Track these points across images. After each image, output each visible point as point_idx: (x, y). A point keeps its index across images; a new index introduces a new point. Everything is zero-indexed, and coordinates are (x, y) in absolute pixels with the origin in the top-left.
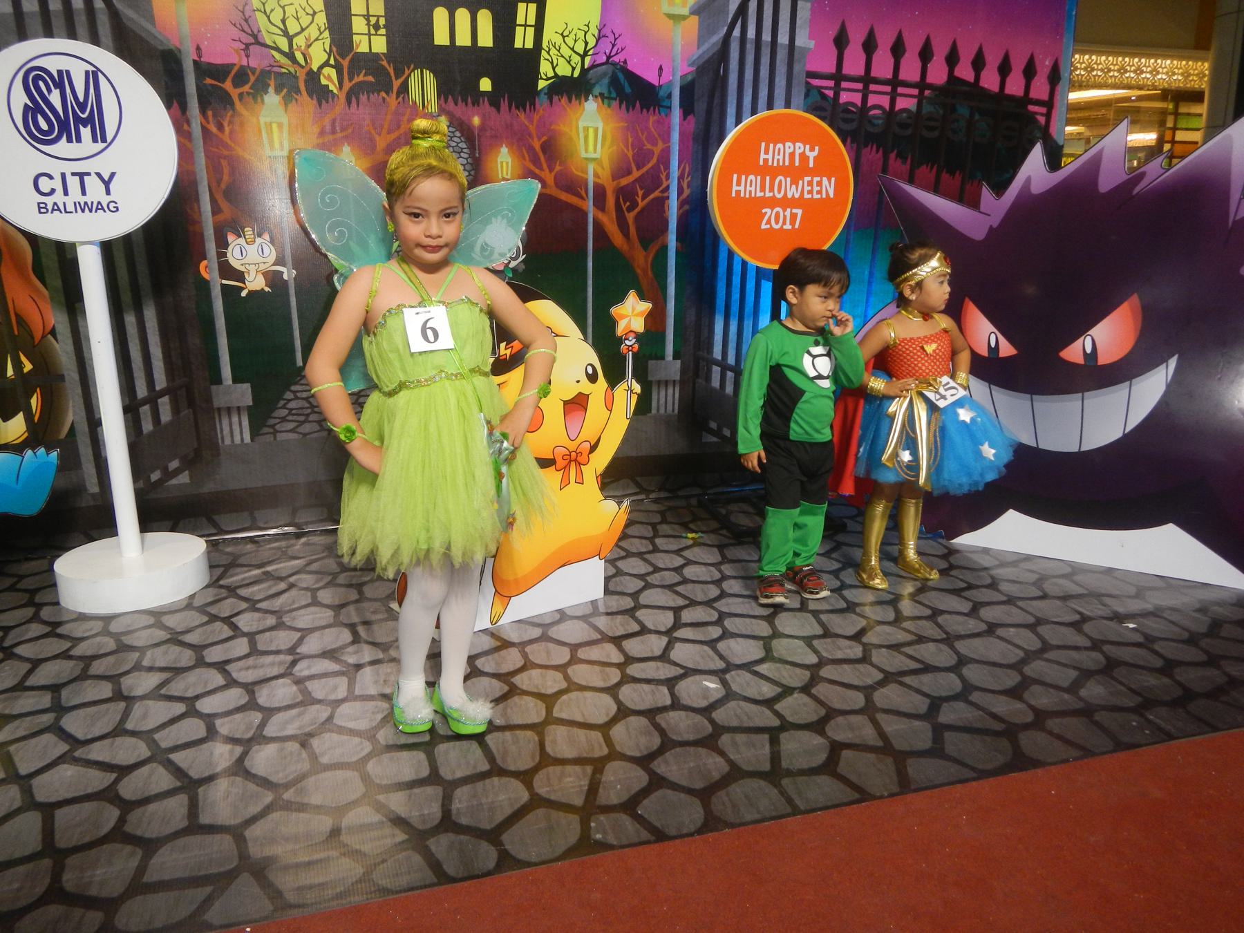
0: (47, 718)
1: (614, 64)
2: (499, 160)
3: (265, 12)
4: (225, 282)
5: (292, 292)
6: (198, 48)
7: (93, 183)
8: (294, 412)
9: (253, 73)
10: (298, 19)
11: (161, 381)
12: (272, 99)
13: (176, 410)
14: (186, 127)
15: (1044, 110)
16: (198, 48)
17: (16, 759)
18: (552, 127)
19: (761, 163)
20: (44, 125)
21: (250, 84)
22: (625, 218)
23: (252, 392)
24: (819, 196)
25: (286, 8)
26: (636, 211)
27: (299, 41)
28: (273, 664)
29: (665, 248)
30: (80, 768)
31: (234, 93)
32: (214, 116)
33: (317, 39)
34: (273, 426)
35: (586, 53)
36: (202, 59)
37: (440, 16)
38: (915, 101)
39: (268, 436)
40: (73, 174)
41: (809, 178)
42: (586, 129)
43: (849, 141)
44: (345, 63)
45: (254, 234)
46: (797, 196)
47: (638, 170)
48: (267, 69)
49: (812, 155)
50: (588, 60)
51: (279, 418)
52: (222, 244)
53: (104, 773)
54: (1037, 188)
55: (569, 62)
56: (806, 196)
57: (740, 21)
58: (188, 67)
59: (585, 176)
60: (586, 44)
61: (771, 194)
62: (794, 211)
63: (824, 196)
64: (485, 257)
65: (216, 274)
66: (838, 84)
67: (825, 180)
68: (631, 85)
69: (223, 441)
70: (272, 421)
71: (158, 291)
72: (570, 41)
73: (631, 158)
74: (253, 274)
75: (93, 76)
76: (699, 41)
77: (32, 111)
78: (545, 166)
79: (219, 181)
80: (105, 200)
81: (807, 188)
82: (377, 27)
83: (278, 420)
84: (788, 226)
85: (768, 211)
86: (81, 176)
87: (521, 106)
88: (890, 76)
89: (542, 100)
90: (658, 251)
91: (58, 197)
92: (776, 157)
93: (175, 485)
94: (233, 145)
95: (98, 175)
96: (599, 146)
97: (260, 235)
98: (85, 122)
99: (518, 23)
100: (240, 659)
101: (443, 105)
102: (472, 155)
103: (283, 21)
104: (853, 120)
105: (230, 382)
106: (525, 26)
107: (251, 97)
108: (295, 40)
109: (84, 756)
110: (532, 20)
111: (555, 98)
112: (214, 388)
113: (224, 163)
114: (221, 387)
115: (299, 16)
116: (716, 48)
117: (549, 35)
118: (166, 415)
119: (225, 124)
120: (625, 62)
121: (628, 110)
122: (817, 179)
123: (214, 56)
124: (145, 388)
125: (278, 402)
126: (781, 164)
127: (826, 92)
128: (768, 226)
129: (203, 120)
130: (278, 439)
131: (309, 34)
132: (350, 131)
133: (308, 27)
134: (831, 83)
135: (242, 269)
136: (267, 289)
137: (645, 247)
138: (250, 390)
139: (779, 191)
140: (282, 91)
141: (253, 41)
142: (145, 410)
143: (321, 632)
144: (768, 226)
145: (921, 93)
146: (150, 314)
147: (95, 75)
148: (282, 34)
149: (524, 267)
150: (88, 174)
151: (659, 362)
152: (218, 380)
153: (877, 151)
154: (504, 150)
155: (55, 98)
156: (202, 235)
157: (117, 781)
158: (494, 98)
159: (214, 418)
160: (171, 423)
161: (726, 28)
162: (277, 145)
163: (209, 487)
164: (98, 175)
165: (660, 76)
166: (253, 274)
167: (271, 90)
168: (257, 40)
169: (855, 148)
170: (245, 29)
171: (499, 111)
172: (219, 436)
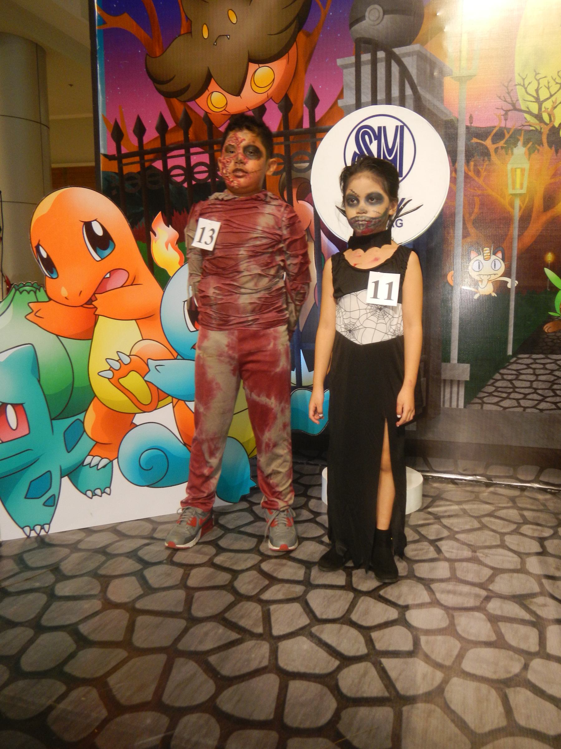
0: (299, 589)
3: (524, 86)
6: (471, 117)
8: (499, 389)
9: (508, 133)
10: (548, 88)
12: (520, 150)
16: (471, 117)
17: (273, 619)
21: (505, 140)
23: (471, 370)
25: (540, 81)
27: (548, 105)
28: (468, 595)
30: (314, 645)
32: (475, 165)
34: (481, 398)
36: (472, 125)
39: (477, 405)
45: (491, 252)
48: (520, 128)
51: (487, 393)
53: (330, 657)
58: (462, 132)
69: (444, 405)
70: (481, 395)
75: (400, 130)
79: (470, 214)
83: (486, 395)
97: (495, 254)
100: (442, 581)
103: (537, 91)
107: (503, 152)
108: (545, 105)
109: (318, 634)
112: (444, 364)
114: (448, 365)
115: (550, 85)
123: (480, 123)
125: (488, 381)
129: (466, 168)
130: (484, 408)
131: (556, 100)
133: (556, 93)
136: (494, 294)
138: (469, 369)
140: (528, 143)
141: (511, 107)
143: (510, 574)
147: (402, 128)
148: (534, 100)
152: (447, 359)
157: (339, 669)
159: (440, 387)
162: (518, 186)
166: (485, 282)
167: (520, 144)
168: (516, 108)
170: (507, 100)
172: (442, 400)
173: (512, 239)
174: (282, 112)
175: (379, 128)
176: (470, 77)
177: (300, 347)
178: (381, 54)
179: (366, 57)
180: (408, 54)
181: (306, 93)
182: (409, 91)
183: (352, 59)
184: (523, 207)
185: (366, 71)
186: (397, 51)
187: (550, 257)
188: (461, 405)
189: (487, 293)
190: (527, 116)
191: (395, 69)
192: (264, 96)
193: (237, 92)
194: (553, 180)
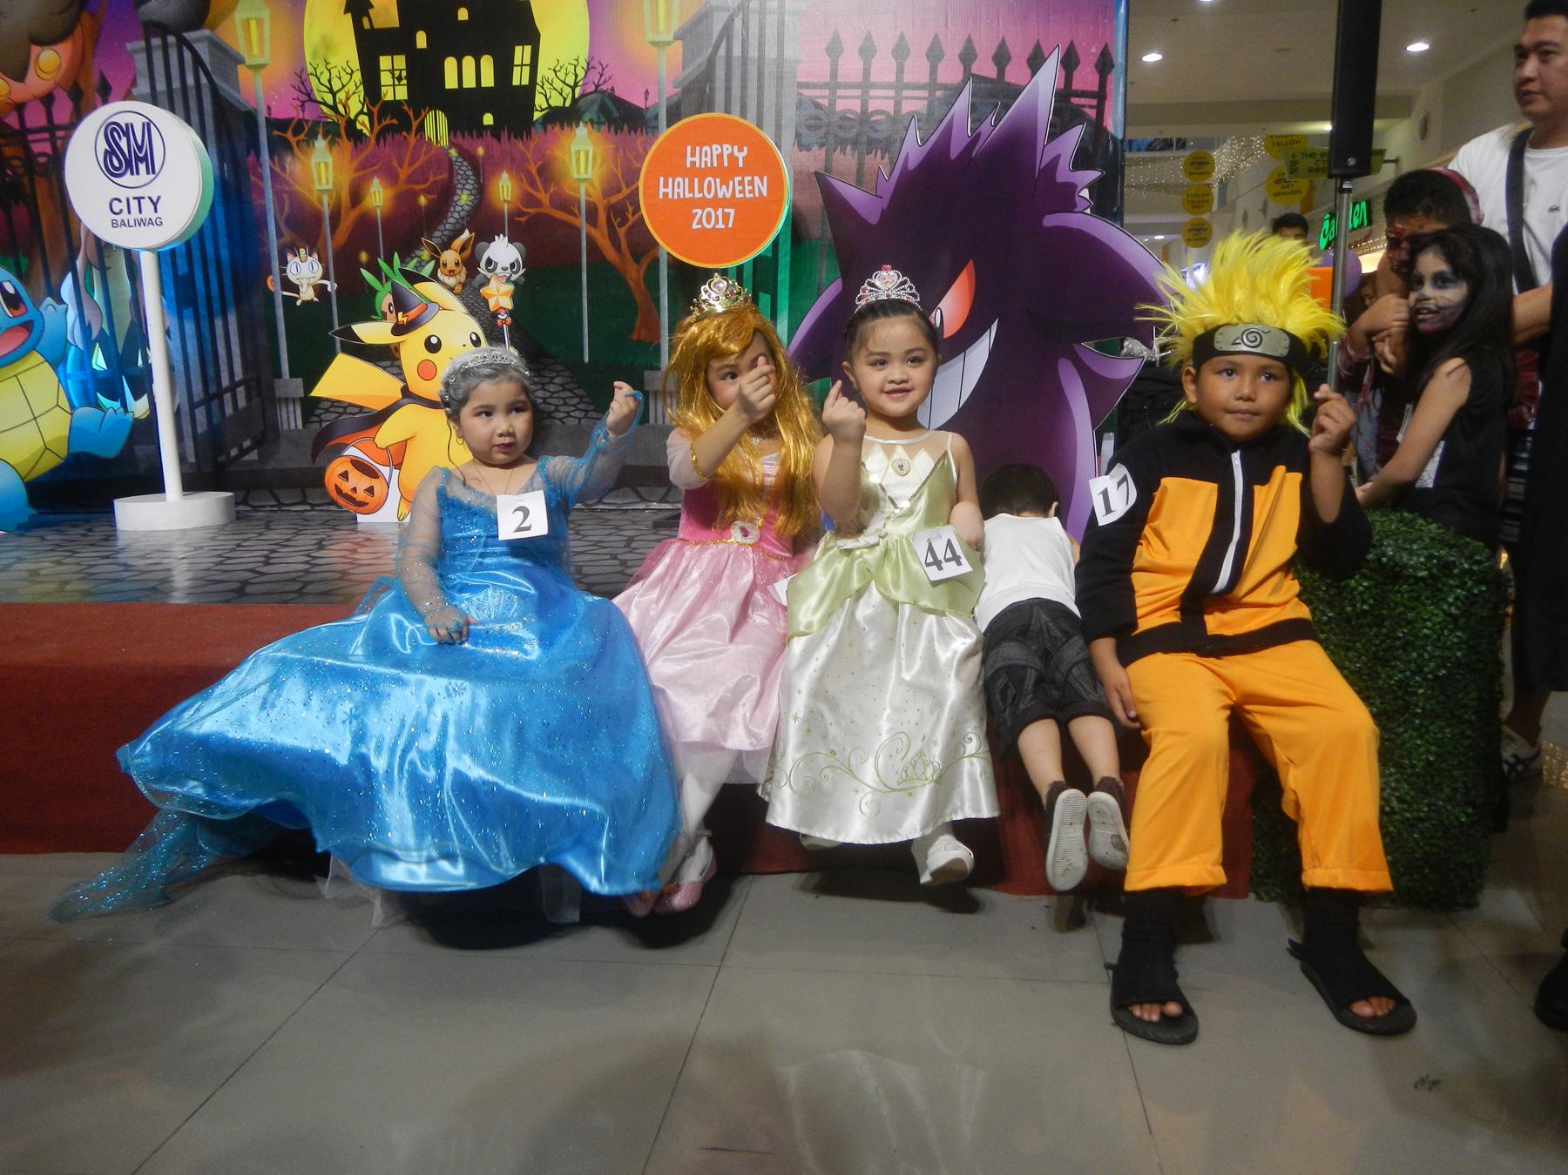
1: (604, 92)
2: (500, 184)
4: (285, 293)
5: (334, 301)
6: (269, 108)
7: (146, 204)
11: (239, 376)
12: (321, 144)
13: (249, 398)
14: (259, 170)
15: (1094, 102)
18: (548, 152)
19: (688, 165)
20: (117, 164)
22: (616, 233)
24: (752, 195)
26: (627, 226)
27: (341, 96)
29: (656, 261)
31: (293, 140)
33: (354, 93)
34: (318, 416)
35: (576, 84)
37: (450, 64)
38: (926, 102)
40: (135, 198)
41: (740, 178)
42: (578, 152)
43: (849, 147)
44: (375, 110)
46: (728, 195)
47: (628, 187)
49: (741, 156)
50: (578, 91)
52: (284, 262)
54: (912, 165)
55: (561, 94)
56: (738, 196)
57: (724, 41)
59: (577, 195)
60: (576, 76)
61: (701, 195)
62: (726, 210)
63: (757, 195)
64: (490, 271)
65: (279, 286)
66: (833, 93)
67: (757, 179)
68: (618, 109)
70: (318, 412)
71: (239, 300)
72: (561, 75)
73: (620, 175)
74: (305, 286)
75: (147, 126)
76: (683, 63)
77: (109, 153)
78: (540, 186)
79: (282, 210)
80: (154, 216)
81: (738, 188)
82: (400, 79)
84: (721, 226)
85: (699, 211)
86: (139, 199)
87: (519, 135)
88: (892, 78)
89: (537, 131)
90: (649, 265)
91: (125, 216)
92: (704, 159)
93: (247, 461)
94: (291, 182)
95: (150, 199)
96: (590, 167)
97: (310, 255)
98: (139, 159)
99: (516, 63)
101: (453, 140)
102: (477, 181)
103: (329, 81)
104: (852, 128)
105: (288, 377)
106: (522, 65)
107: (303, 145)
108: (338, 95)
110: (527, 60)
111: (549, 127)
112: (276, 380)
113: (285, 196)
116: (702, 69)
117: (543, 71)
118: (242, 403)
119: (287, 166)
120: (613, 89)
121: (616, 133)
122: (747, 179)
123: (279, 114)
124: (227, 379)
126: (709, 165)
127: (821, 101)
128: (700, 226)
132: (377, 167)
134: (827, 92)
135: (297, 282)
136: (316, 299)
137: (637, 261)
139: (709, 192)
142: (227, 396)
144: (700, 226)
145: (932, 93)
146: (232, 318)
147: (148, 125)
149: (523, 280)
150: (143, 198)
151: (654, 372)
152: (279, 375)
153: (882, 158)
154: (505, 175)
155: (123, 143)
156: (269, 255)
158: (495, 131)
160: (245, 409)
161: (711, 49)
162: (324, 180)
163: (271, 465)
164: (150, 199)
165: (646, 99)
166: (305, 286)
167: (320, 136)
169: (856, 155)
171: (499, 139)
173: (325, 236)
174: (72, 99)
175: (127, 125)
176: (262, 66)
177: (122, 373)
178: (171, 39)
179: (156, 42)
180: (199, 40)
181: (95, 80)
182: (204, 80)
183: (142, 44)
184: (332, 203)
185: (158, 56)
186: (189, 35)
187: (364, 257)
188: (300, 426)
189: (309, 299)
190: (322, 106)
191: (187, 55)
192: (52, 82)
193: (19, 75)
194: (356, 175)
